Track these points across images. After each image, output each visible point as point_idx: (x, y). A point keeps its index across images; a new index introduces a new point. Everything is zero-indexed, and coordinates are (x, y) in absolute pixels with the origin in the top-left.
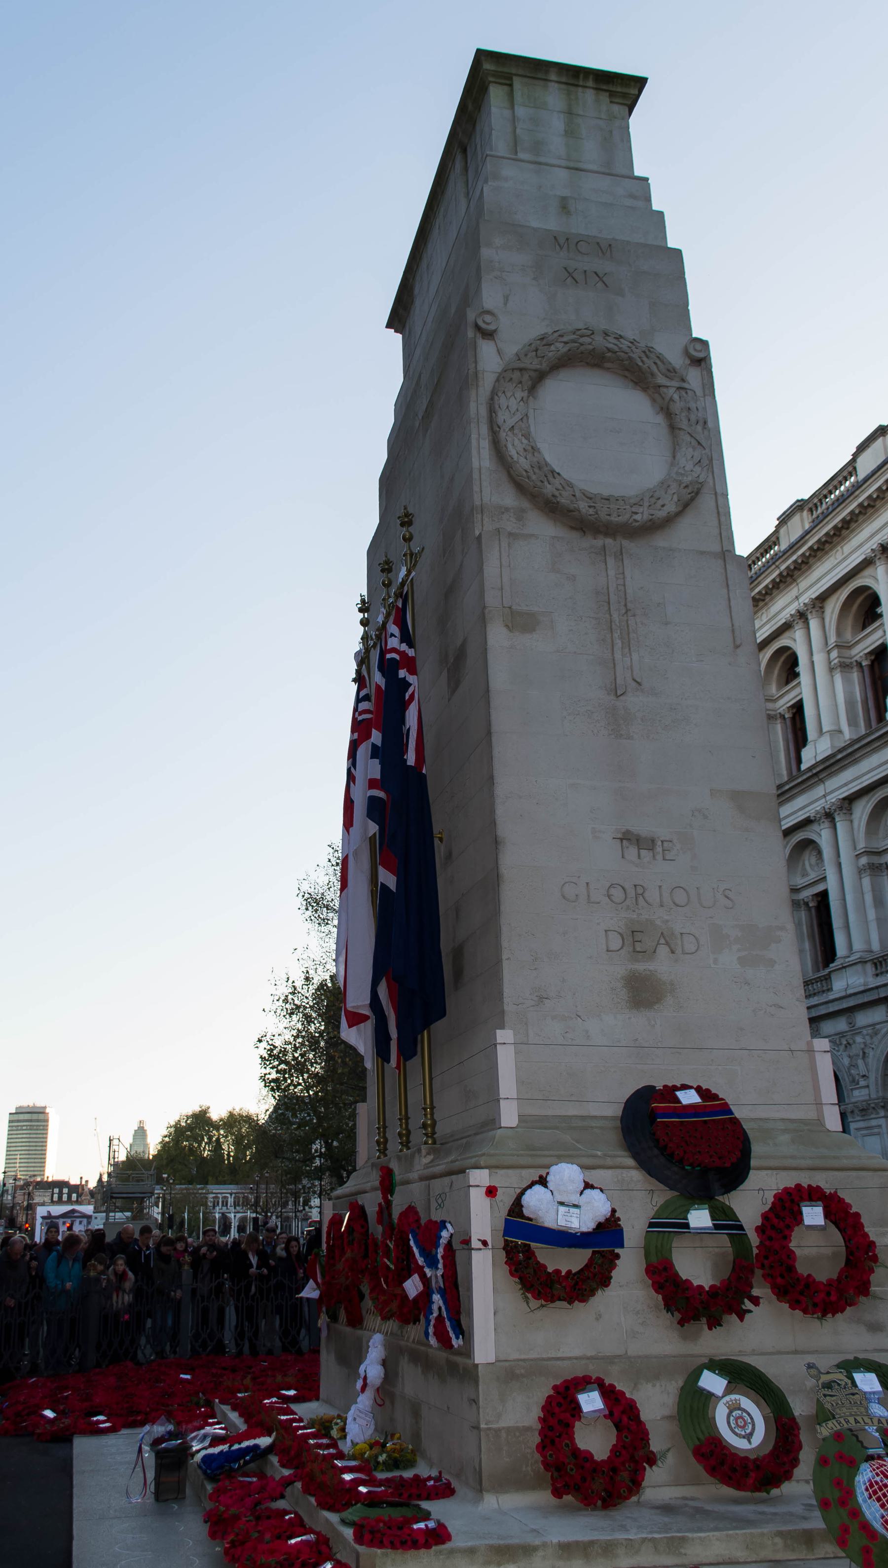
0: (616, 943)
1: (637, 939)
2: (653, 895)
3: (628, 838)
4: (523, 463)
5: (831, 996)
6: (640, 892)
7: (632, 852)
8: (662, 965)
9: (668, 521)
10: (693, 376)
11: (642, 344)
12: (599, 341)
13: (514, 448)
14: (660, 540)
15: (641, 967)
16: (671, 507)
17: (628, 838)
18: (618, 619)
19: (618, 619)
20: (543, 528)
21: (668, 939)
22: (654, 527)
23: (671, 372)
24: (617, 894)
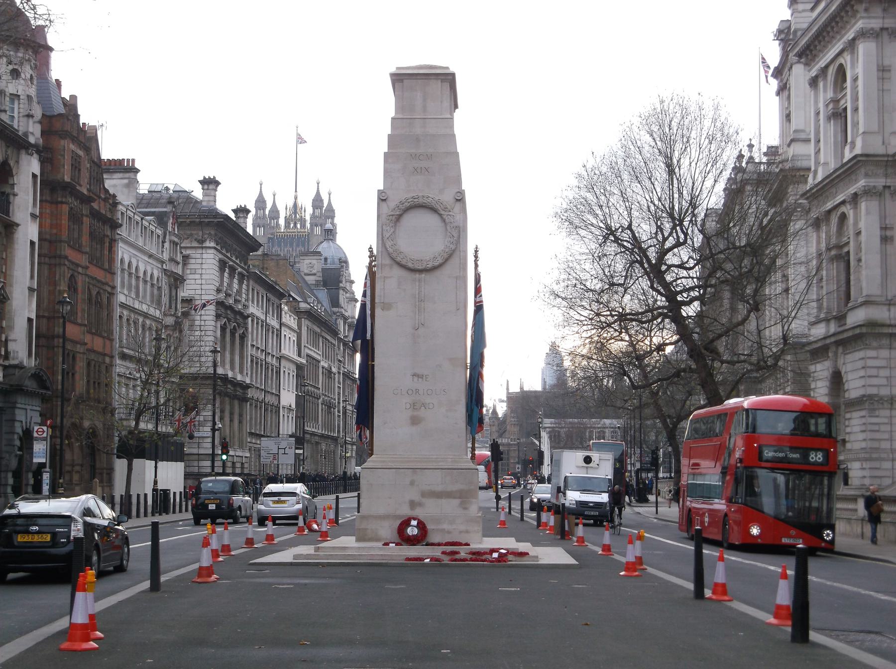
0: (408, 406)
1: (414, 406)
2: (421, 392)
3: (414, 375)
4: (390, 250)
5: (847, 327)
6: (417, 391)
7: (416, 379)
8: (422, 413)
9: (440, 266)
10: (458, 205)
11: (437, 198)
12: (421, 201)
13: (388, 244)
14: (438, 273)
15: (415, 413)
16: (440, 261)
17: (414, 375)
18: (419, 302)
19: (419, 302)
20: (398, 272)
21: (424, 405)
22: (434, 268)
23: (445, 209)
24: (410, 392)
